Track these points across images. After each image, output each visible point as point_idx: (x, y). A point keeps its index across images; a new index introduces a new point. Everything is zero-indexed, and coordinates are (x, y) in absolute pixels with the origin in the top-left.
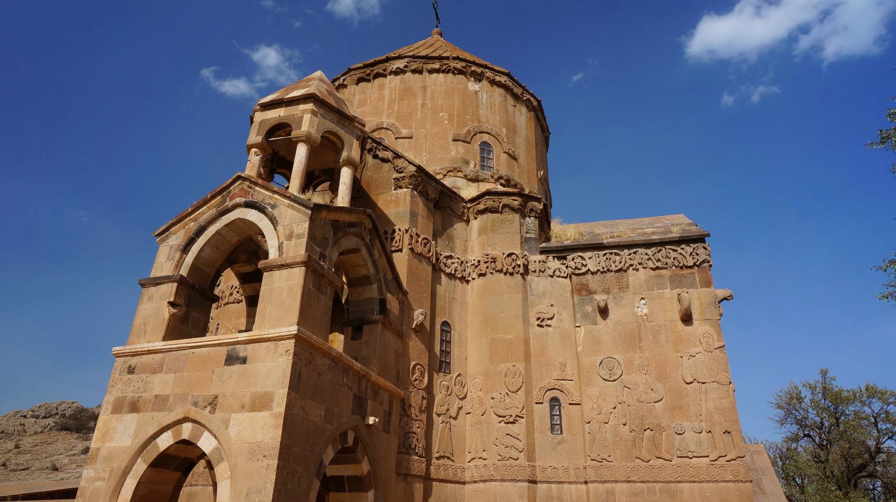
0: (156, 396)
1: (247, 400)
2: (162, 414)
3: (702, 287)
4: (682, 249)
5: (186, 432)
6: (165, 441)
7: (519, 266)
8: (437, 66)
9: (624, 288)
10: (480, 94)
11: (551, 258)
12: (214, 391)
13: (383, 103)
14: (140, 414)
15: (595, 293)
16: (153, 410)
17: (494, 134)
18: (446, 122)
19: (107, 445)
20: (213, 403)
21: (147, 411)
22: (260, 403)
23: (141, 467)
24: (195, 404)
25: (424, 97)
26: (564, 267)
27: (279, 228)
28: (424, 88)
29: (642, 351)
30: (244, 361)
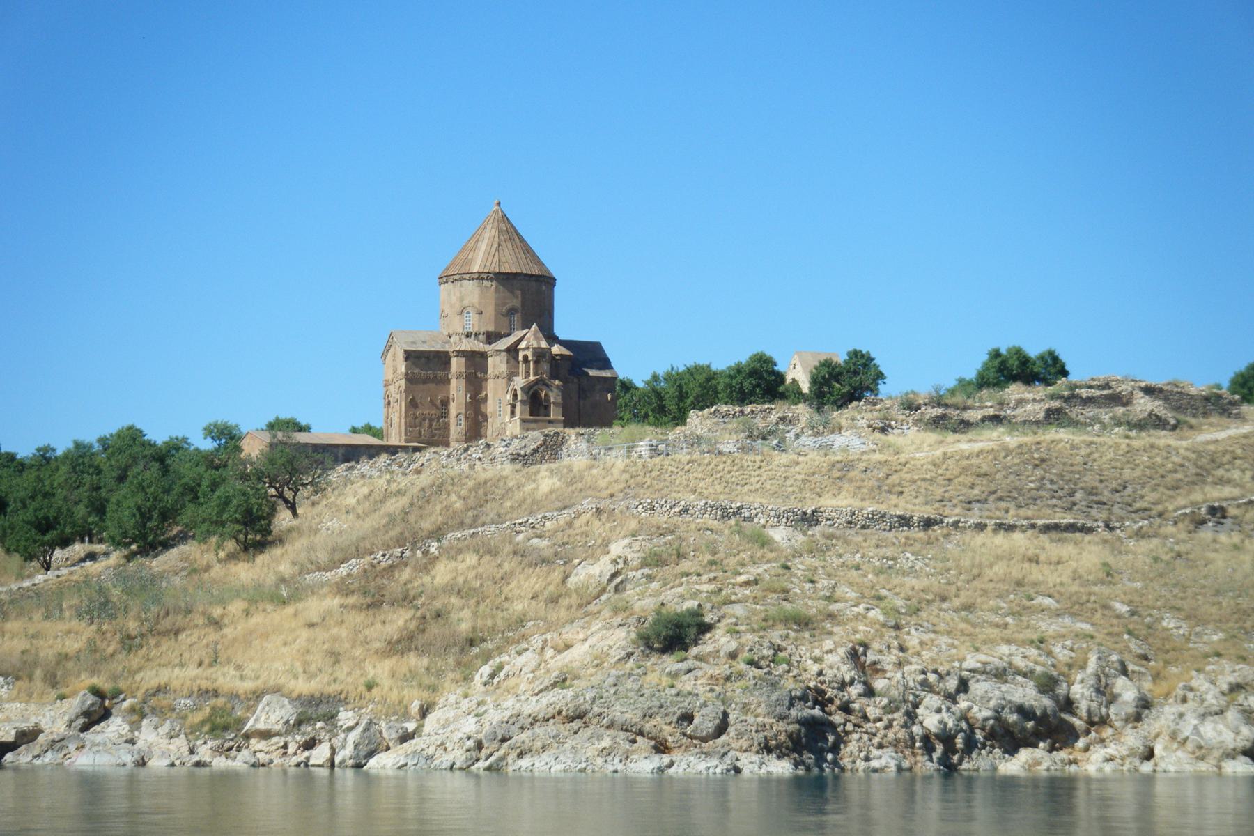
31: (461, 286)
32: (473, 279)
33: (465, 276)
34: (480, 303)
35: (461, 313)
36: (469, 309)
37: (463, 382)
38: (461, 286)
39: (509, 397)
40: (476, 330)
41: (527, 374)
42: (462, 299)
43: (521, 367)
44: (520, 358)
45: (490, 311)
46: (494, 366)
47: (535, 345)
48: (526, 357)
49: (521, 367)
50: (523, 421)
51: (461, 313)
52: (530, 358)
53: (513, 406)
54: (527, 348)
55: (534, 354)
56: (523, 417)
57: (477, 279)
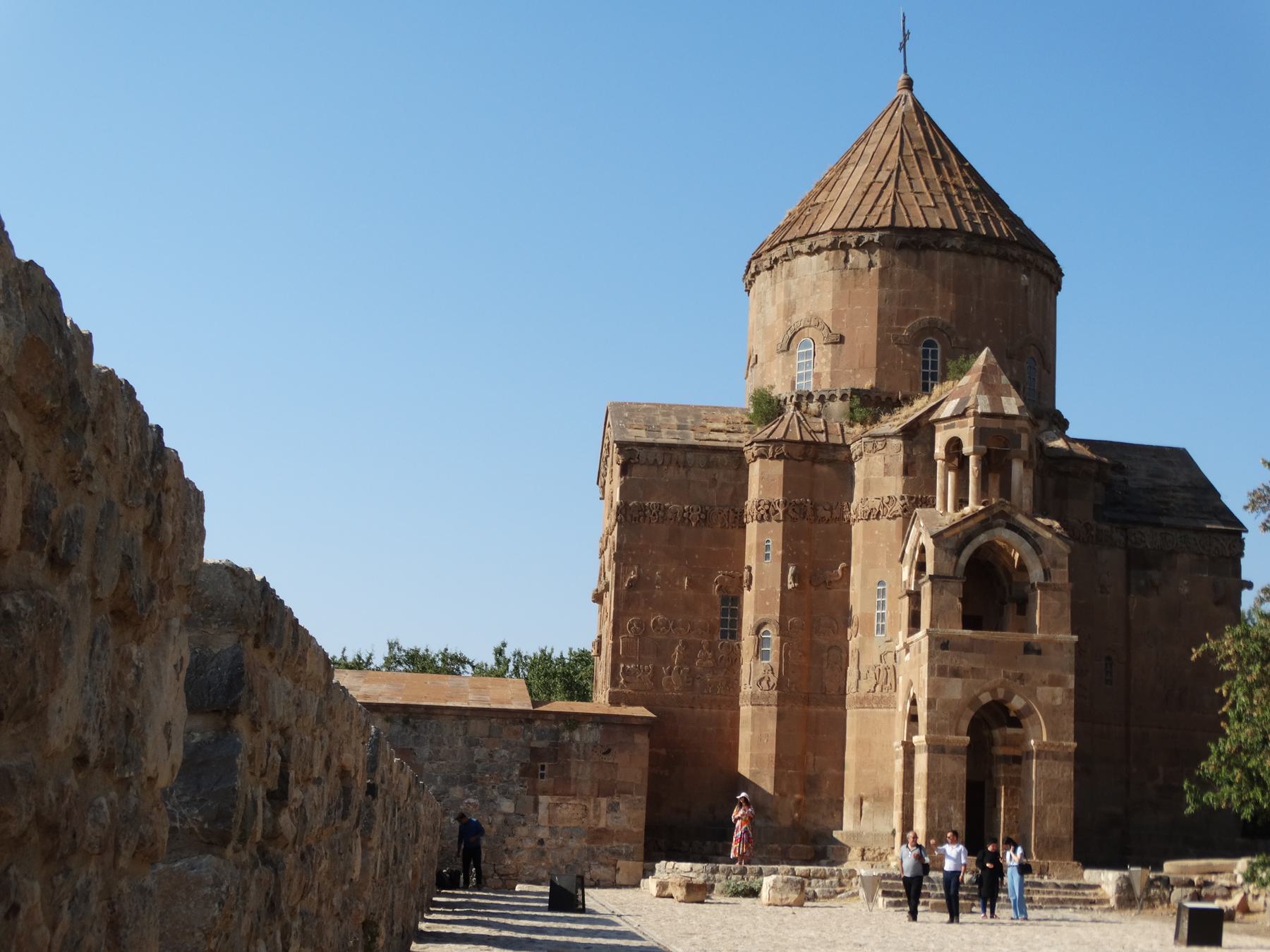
4: (1223, 540)
5: (1001, 694)
6: (986, 698)
22: (1055, 681)
27: (1044, 555)
31: (790, 274)
32: (819, 250)
33: (797, 246)
34: (836, 315)
35: (787, 347)
36: (810, 332)
37: (775, 531)
38: (790, 274)
39: (906, 573)
40: (826, 385)
41: (961, 502)
42: (790, 310)
43: (945, 480)
44: (939, 451)
45: (865, 333)
46: (867, 486)
47: (984, 406)
48: (954, 445)
49: (945, 480)
50: (940, 644)
51: (787, 347)
52: (967, 448)
53: (915, 597)
54: (960, 415)
55: (981, 434)
56: (940, 630)
57: (833, 246)
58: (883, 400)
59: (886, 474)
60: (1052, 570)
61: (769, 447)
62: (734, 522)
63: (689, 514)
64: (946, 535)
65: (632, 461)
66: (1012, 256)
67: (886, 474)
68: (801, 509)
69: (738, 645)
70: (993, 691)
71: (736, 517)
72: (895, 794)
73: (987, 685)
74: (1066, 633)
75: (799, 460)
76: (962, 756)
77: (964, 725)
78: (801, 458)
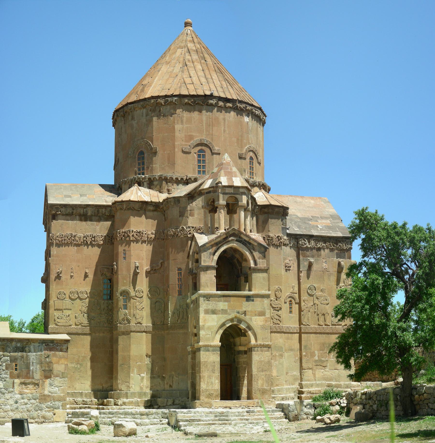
0: (222, 310)
1: (257, 313)
2: (226, 315)
3: (347, 259)
7: (281, 242)
8: (231, 105)
9: (319, 256)
10: (249, 123)
11: (292, 238)
12: (244, 309)
13: (203, 125)
14: (218, 315)
15: (308, 257)
16: (222, 314)
17: (255, 151)
18: (236, 144)
19: (207, 324)
20: (245, 313)
21: (220, 314)
23: (221, 332)
24: (238, 313)
25: (225, 125)
26: (296, 243)
28: (224, 119)
29: (323, 284)
30: (253, 301)
58: (179, 179)
59: (180, 216)
60: (258, 260)
61: (123, 204)
62: (109, 242)
63: (86, 238)
64: (207, 245)
65: (58, 213)
66: (240, 107)
67: (180, 216)
68: (140, 235)
69: (112, 302)
70: (232, 320)
71: (109, 239)
72: (189, 372)
73: (230, 317)
74: (266, 290)
75: (139, 211)
76: (218, 352)
77: (218, 337)
78: (139, 209)
